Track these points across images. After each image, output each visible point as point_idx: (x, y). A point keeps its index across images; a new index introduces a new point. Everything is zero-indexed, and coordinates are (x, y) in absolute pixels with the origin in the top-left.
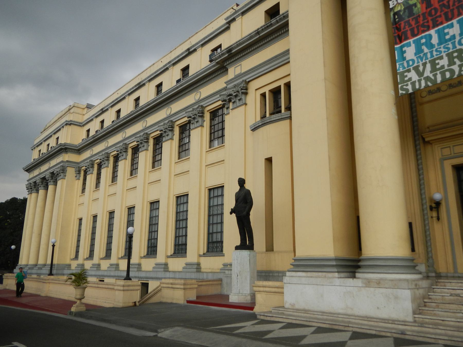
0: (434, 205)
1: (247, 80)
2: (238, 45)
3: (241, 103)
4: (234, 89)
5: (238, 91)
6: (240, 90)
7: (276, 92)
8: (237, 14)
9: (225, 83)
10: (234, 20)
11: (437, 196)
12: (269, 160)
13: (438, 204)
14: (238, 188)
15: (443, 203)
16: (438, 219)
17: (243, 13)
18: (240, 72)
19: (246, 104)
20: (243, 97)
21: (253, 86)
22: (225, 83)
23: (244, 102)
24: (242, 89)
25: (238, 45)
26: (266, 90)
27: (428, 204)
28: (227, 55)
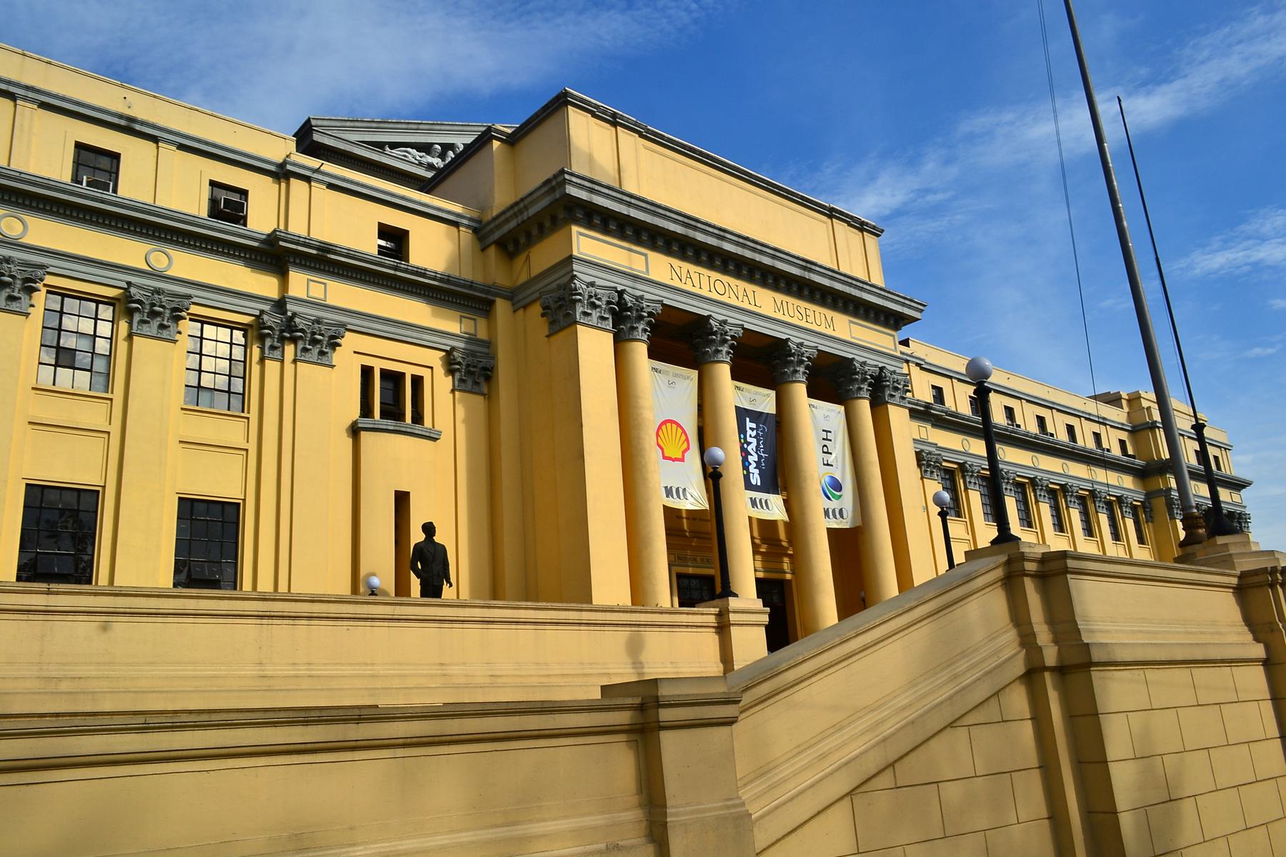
1: (349, 327)
7: (394, 379)
8: (321, 177)
10: (307, 179)
21: (350, 341)
26: (378, 365)
28: (314, 252)
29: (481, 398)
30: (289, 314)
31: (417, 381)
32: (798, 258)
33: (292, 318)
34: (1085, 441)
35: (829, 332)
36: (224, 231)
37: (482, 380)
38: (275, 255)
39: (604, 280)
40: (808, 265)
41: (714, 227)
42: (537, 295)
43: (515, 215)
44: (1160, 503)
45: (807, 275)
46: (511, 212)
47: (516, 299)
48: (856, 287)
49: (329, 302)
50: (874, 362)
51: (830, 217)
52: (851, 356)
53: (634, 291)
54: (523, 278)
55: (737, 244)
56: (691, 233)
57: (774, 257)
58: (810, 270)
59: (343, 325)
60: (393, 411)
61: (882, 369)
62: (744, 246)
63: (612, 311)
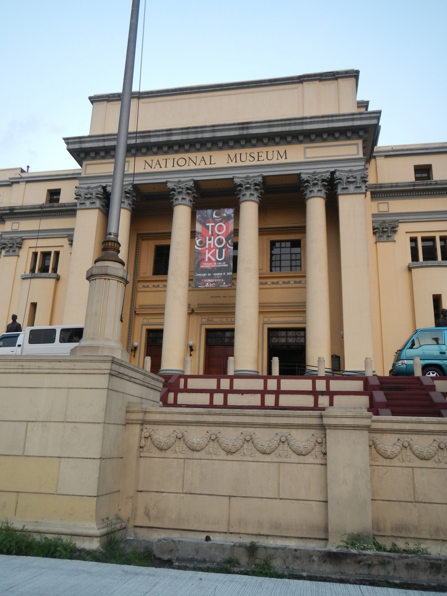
0: (133, 349)
1: (24, 238)
2: (20, 209)
3: (14, 254)
4: (10, 241)
5: (13, 244)
6: (15, 243)
7: (46, 255)
8: (22, 180)
9: (1, 232)
10: (18, 182)
11: (136, 344)
12: (34, 305)
13: (136, 348)
14: (11, 321)
15: (138, 348)
16: (134, 356)
17: (27, 182)
18: (17, 228)
19: (18, 256)
20: (17, 250)
21: (28, 244)
22: (1, 232)
23: (17, 254)
24: (17, 244)
25: (20, 209)
26: (39, 251)
27: (131, 348)
28: (8, 212)
32: (234, 124)
35: (283, 161)
40: (244, 125)
41: (162, 131)
45: (245, 132)
48: (295, 124)
49: (20, 230)
50: (324, 171)
51: (301, 82)
52: (298, 172)
55: (183, 134)
56: (147, 140)
57: (214, 131)
58: (248, 128)
60: (44, 269)
61: (333, 173)
62: (188, 133)
63: (98, 197)
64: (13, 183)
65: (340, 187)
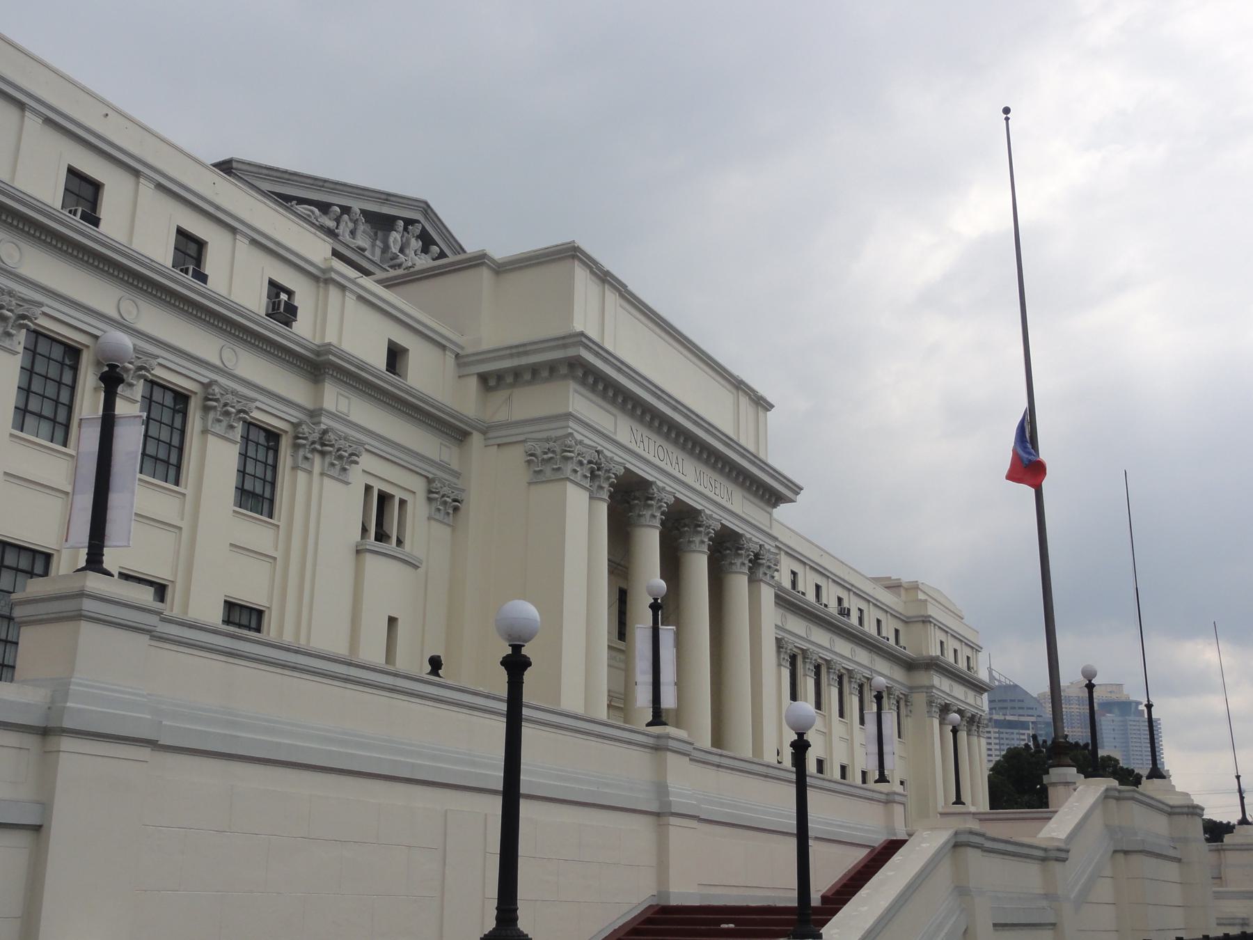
7: (384, 498)
10: (343, 288)
26: (378, 486)
29: (449, 530)
30: (323, 427)
31: (403, 503)
33: (325, 432)
34: (870, 628)
36: (273, 330)
37: (451, 511)
38: (317, 366)
39: (591, 440)
42: (522, 438)
43: (511, 356)
44: (919, 699)
46: (508, 352)
47: (491, 435)
53: (610, 451)
54: (501, 416)
59: (362, 444)
64: (328, 281)
65: (762, 570)
